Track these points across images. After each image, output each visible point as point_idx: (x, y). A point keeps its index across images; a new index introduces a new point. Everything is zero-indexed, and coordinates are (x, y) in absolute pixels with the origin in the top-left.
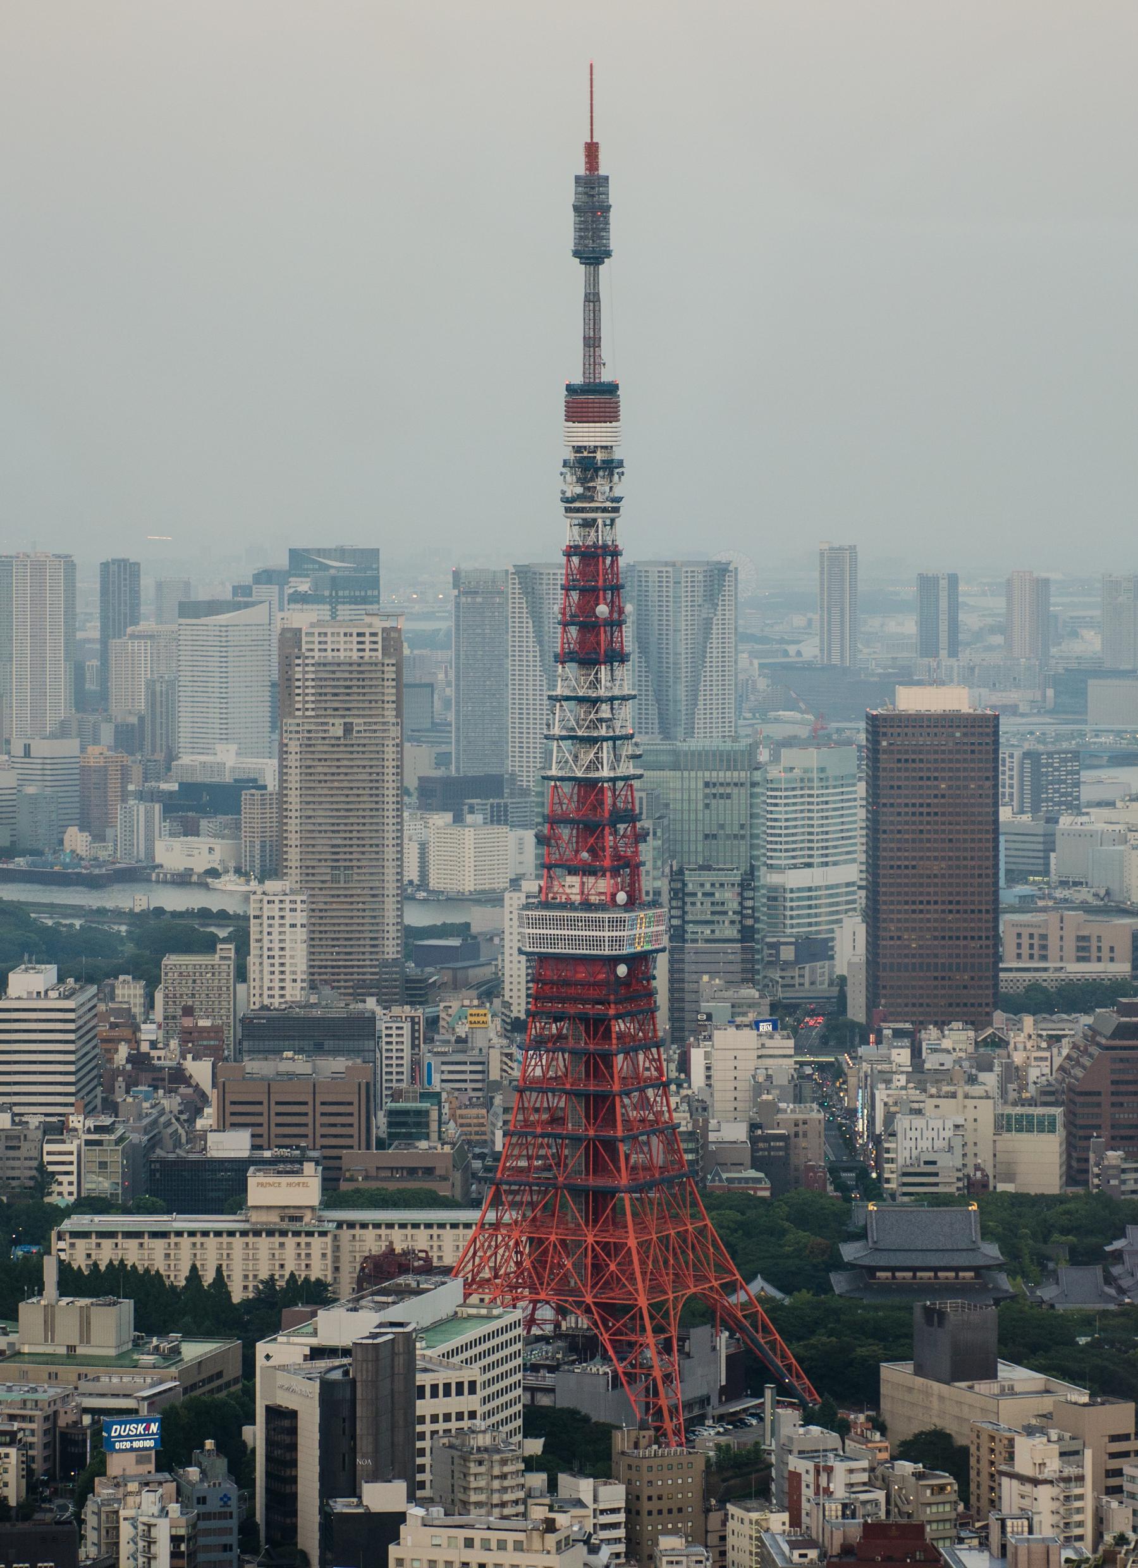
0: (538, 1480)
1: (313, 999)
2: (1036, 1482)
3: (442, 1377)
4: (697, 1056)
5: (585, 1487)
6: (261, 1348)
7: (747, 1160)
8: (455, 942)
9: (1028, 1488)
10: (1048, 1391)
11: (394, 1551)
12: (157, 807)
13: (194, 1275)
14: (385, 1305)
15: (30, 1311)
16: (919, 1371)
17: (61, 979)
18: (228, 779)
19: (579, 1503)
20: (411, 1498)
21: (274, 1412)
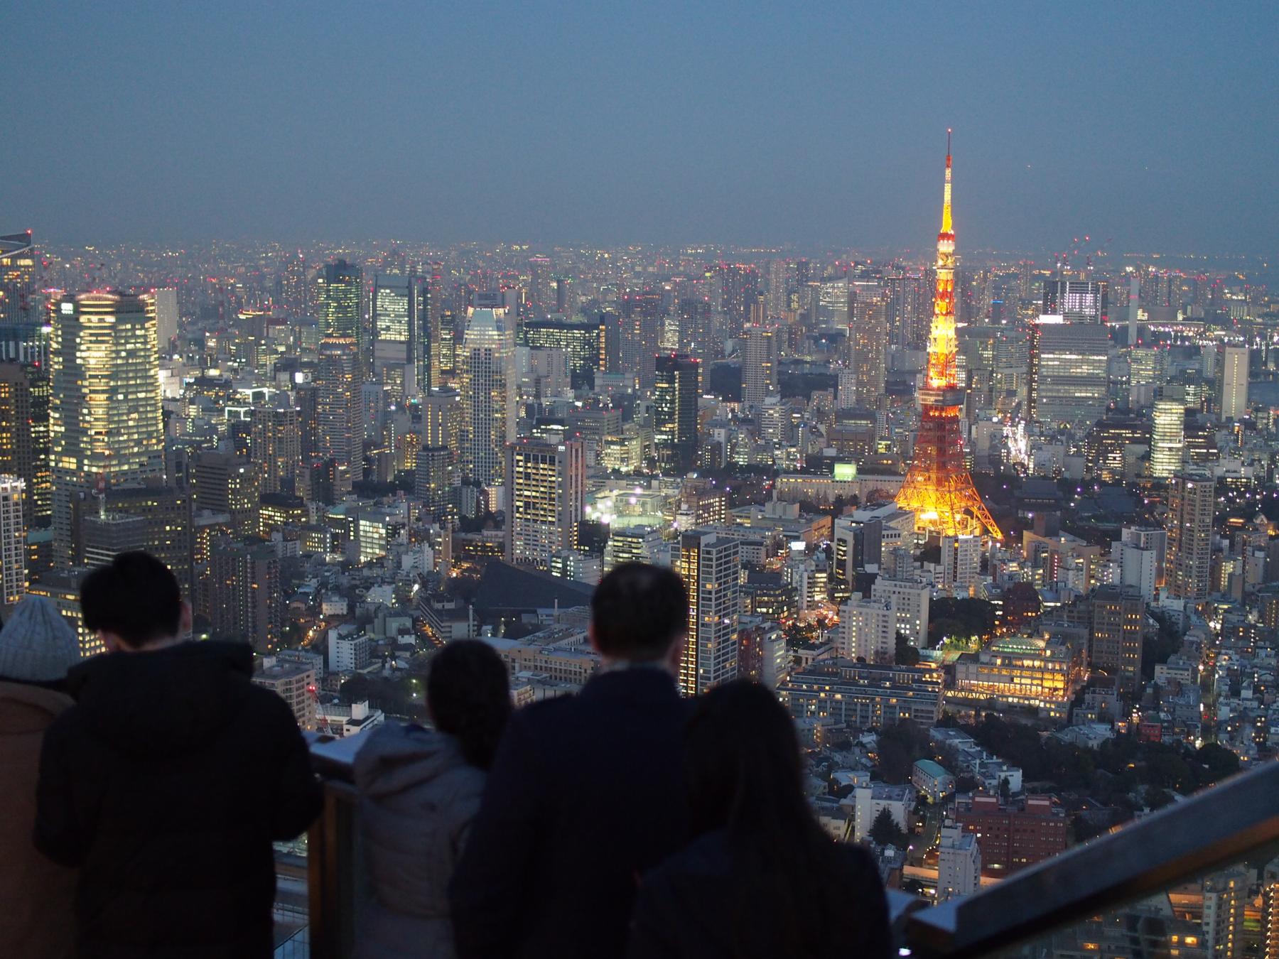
0: (918, 564)
1: (857, 407)
2: (1068, 570)
3: (890, 532)
4: (974, 428)
5: (932, 565)
6: (836, 520)
7: (987, 462)
8: (901, 388)
9: (1066, 571)
10: (1074, 541)
11: (873, 587)
12: (812, 341)
13: (818, 494)
14: (874, 509)
15: (769, 506)
16: (1035, 533)
17: (781, 399)
18: (834, 332)
19: (930, 571)
20: (879, 569)
21: (839, 540)
